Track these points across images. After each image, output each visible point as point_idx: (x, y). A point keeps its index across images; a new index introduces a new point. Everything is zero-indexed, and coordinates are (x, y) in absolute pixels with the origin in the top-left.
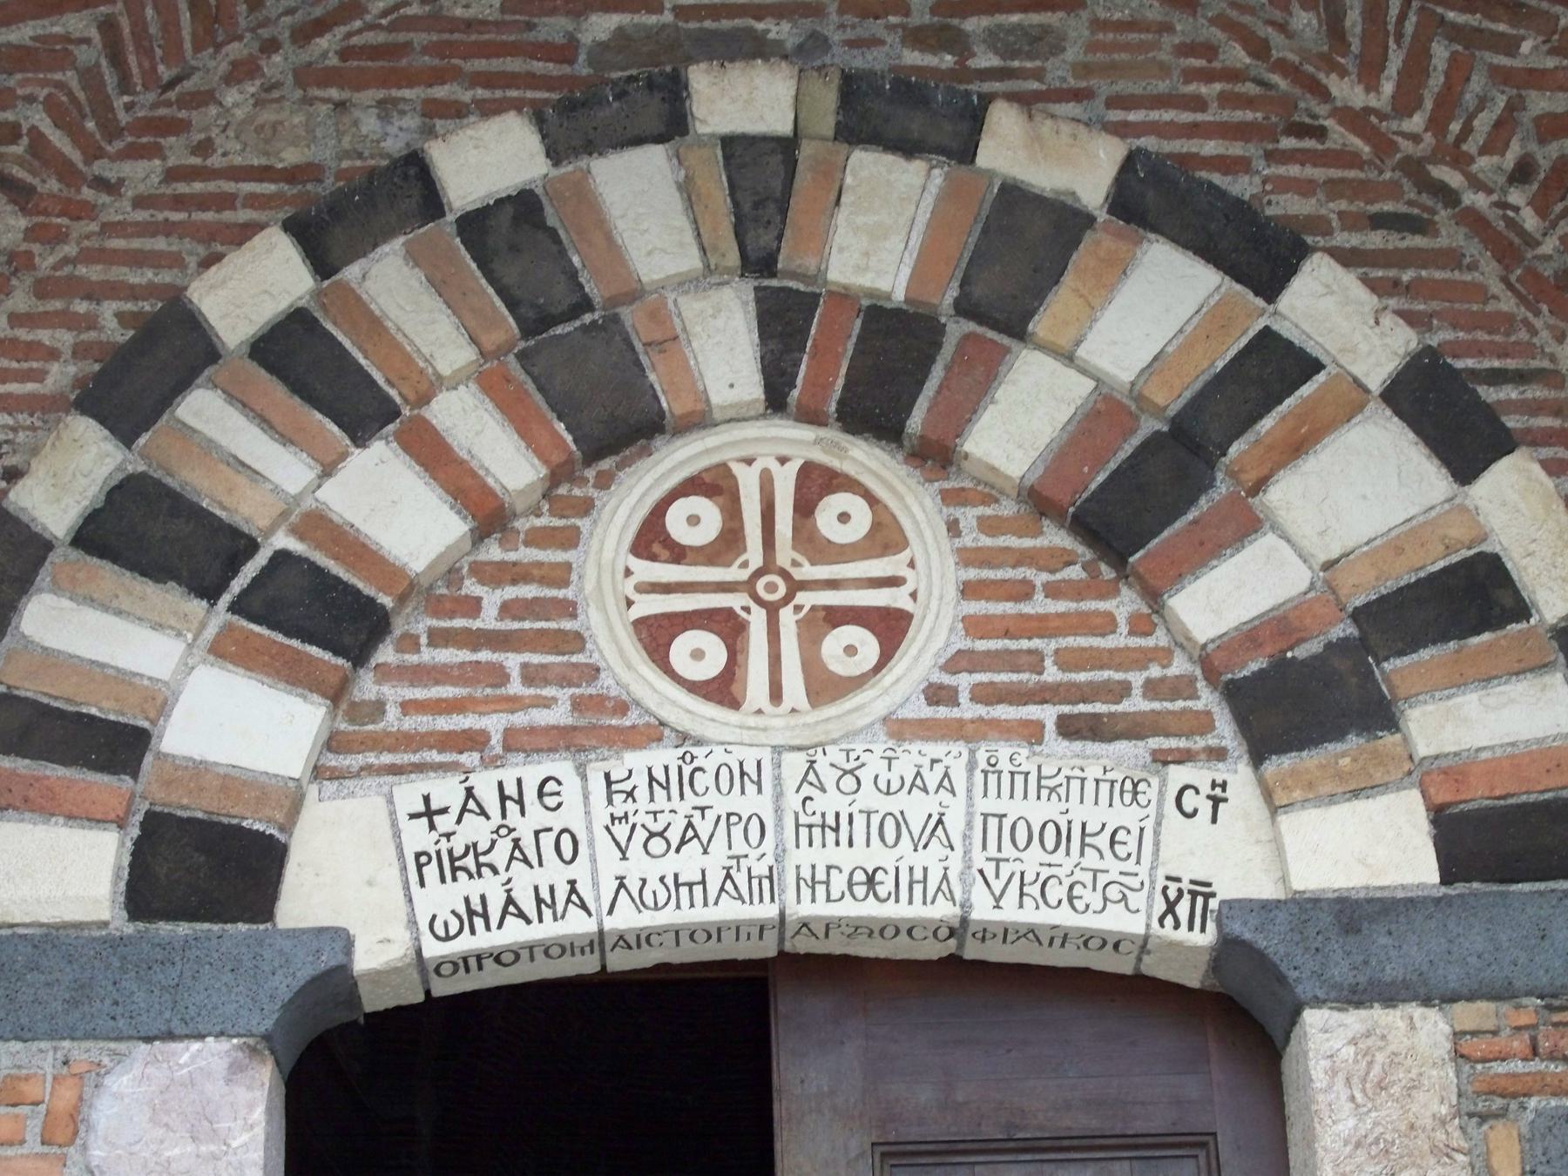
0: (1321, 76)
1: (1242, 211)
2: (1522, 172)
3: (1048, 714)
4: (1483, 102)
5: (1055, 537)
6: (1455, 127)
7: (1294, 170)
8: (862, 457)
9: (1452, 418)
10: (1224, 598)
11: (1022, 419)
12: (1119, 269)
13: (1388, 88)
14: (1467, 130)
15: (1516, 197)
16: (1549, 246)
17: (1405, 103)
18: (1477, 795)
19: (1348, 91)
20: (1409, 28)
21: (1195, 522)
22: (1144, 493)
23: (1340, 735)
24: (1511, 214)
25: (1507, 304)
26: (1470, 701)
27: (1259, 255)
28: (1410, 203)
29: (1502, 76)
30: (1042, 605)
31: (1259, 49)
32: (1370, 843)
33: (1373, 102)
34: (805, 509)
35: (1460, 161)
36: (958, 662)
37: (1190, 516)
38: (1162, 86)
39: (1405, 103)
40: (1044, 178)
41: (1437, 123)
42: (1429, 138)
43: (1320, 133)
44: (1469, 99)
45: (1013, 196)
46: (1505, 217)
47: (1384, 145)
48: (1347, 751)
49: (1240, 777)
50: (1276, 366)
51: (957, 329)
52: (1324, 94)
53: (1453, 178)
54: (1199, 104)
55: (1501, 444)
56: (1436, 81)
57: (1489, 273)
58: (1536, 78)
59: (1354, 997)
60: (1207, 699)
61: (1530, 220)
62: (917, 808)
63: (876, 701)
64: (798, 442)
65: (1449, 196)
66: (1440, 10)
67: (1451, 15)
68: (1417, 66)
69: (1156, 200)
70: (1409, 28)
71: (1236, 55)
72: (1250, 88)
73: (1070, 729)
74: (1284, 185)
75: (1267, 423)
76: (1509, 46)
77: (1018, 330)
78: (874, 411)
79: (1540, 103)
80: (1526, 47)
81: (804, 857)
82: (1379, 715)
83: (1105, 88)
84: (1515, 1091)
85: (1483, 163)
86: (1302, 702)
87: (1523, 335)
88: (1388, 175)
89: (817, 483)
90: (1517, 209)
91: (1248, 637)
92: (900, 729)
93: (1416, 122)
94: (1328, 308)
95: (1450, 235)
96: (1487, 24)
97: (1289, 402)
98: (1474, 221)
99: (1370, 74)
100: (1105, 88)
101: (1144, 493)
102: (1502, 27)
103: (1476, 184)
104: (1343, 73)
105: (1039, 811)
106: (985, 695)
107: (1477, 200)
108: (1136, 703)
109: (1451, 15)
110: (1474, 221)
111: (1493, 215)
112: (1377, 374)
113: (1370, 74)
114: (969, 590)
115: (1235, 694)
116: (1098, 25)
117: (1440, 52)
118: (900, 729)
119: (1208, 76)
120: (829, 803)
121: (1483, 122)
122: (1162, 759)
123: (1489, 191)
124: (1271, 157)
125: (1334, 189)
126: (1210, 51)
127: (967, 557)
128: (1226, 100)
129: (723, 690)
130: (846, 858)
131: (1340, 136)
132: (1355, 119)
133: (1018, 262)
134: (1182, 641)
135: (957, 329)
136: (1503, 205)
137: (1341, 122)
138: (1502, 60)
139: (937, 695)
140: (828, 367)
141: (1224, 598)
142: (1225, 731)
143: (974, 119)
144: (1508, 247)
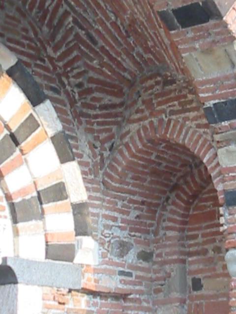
0: (46, 45)
2: (80, 85)
4: (78, 67)
6: (69, 69)
7: (39, 70)
13: (58, 54)
14: (72, 70)
15: (76, 90)
16: (79, 104)
17: (60, 59)
18: (53, 242)
19: (50, 50)
20: (71, 45)
21: (13, 160)
23: (31, 220)
24: (74, 94)
25: (70, 117)
28: (57, 85)
29: (86, 65)
31: (36, 34)
33: (54, 56)
35: (68, 77)
37: (12, 157)
38: (17, 38)
39: (60, 59)
41: (66, 66)
42: (63, 70)
43: (43, 61)
44: (76, 65)
46: (72, 94)
47: (55, 68)
52: (45, 49)
53: (64, 79)
54: (23, 45)
56: (70, 58)
61: (77, 97)
65: (64, 85)
66: (80, 45)
67: (82, 48)
70: (71, 45)
71: (32, 35)
72: (33, 44)
74: (40, 75)
75: (29, 139)
76: (92, 60)
79: (91, 74)
80: (95, 62)
85: (72, 80)
87: (72, 126)
88: (54, 76)
90: (75, 93)
93: (61, 64)
95: (63, 97)
96: (89, 53)
97: (34, 134)
99: (56, 49)
102: (92, 55)
103: (69, 84)
104: (50, 46)
107: (68, 88)
109: (82, 48)
110: (67, 93)
111: (71, 93)
112: (51, 133)
113: (56, 49)
116: (8, 16)
117: (75, 53)
119: (26, 38)
121: (76, 71)
123: (71, 87)
124: (37, 66)
125: (46, 78)
126: (25, 30)
128: (30, 47)
131: (48, 64)
132: (51, 59)
136: (73, 91)
137: (48, 60)
138: (88, 62)
144: (73, 103)
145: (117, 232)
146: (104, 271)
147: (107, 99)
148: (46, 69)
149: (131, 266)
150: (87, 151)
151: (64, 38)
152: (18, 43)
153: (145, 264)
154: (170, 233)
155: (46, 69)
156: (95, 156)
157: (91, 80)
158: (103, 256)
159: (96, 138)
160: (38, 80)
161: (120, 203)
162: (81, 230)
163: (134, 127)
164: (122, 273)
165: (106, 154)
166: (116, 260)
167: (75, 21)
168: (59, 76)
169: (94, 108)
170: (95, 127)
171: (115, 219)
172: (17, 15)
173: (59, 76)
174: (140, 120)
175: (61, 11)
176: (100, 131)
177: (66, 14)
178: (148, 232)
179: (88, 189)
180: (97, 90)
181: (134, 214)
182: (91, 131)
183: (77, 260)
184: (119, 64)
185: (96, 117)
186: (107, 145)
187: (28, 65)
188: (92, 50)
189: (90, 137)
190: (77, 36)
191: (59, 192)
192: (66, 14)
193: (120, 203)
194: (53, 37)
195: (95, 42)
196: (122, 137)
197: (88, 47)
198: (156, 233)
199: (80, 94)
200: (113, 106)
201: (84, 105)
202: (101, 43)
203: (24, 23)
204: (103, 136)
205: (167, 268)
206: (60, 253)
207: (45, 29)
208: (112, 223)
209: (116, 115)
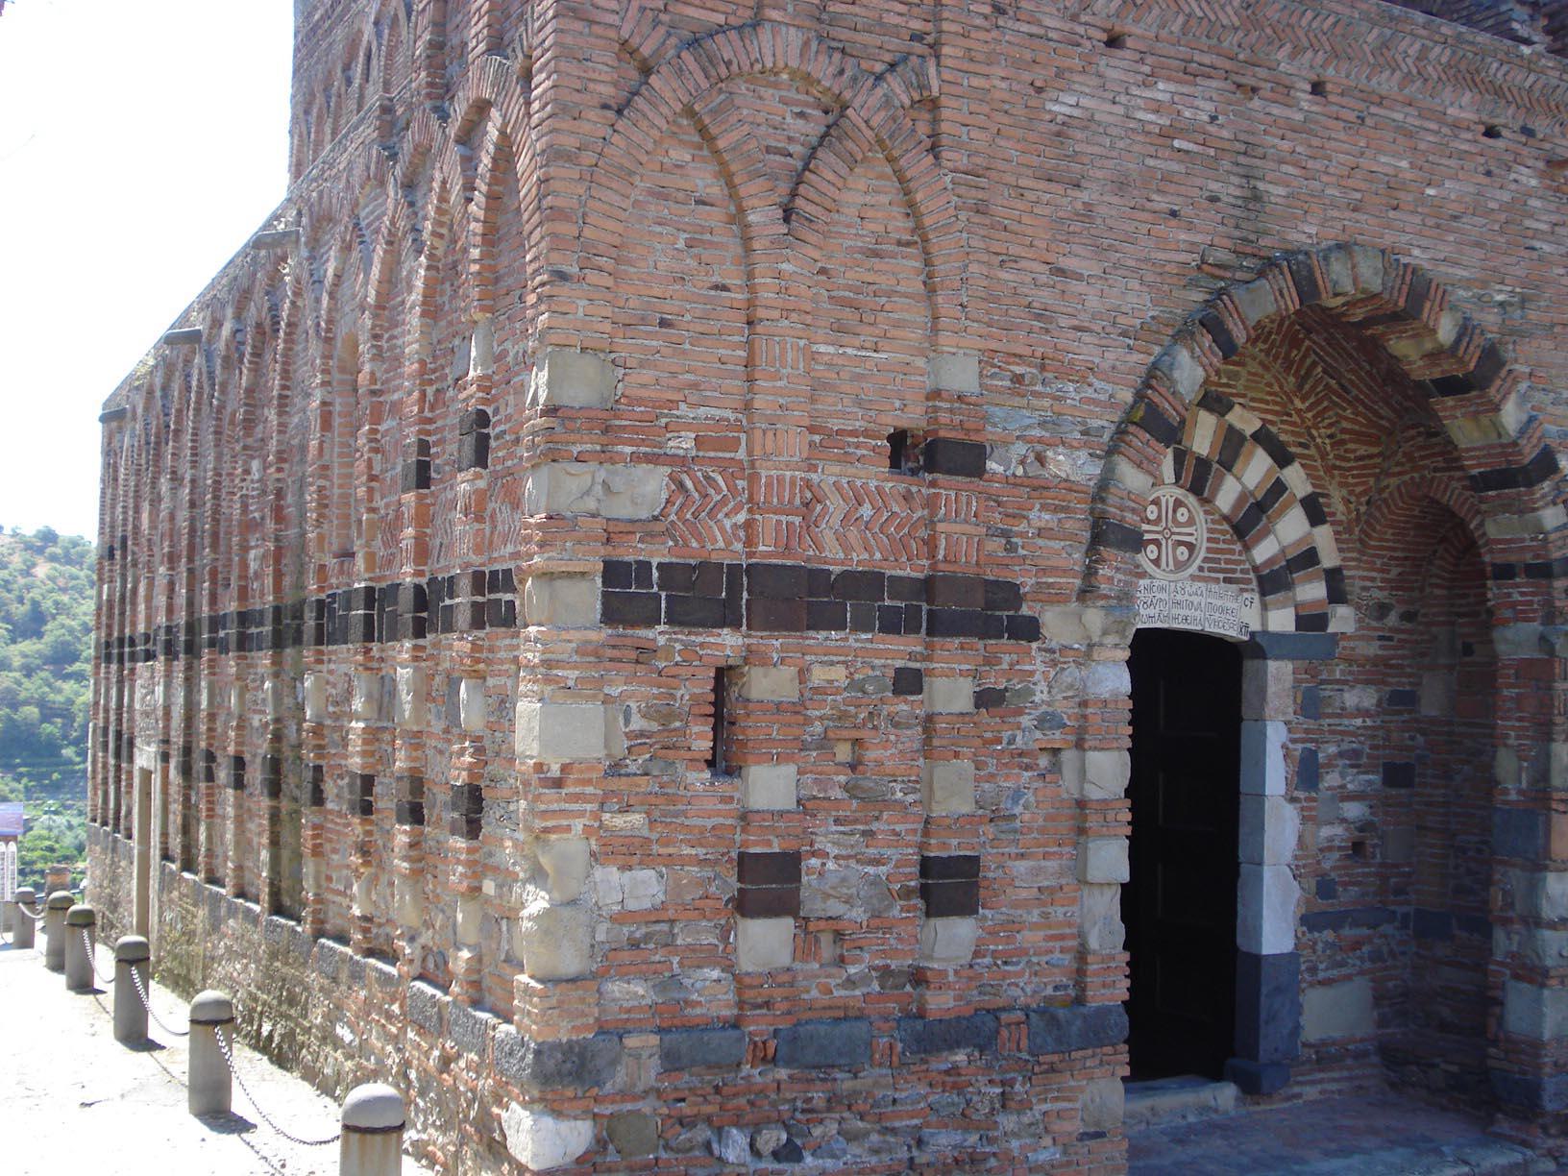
1: (1282, 446)
2: (1330, 436)
3: (1221, 576)
5: (1226, 527)
8: (1191, 500)
9: (1315, 511)
10: (1264, 551)
11: (1227, 495)
12: (1251, 454)
17: (1309, 409)
22: (1249, 520)
26: (1308, 587)
27: (1282, 458)
30: (1222, 546)
31: (1281, 387)
32: (1282, 620)
34: (1175, 511)
36: (1206, 560)
38: (1260, 395)
39: (1309, 409)
40: (1238, 425)
45: (1231, 427)
48: (1280, 596)
49: (1256, 597)
50: (1278, 488)
51: (1216, 466)
54: (1267, 402)
55: (1324, 522)
57: (1318, 463)
58: (1346, 419)
59: (1277, 658)
60: (1252, 575)
62: (1196, 599)
63: (1193, 569)
64: (1179, 493)
65: (1313, 438)
68: (1318, 402)
69: (1262, 438)
71: (1276, 388)
73: (1227, 580)
74: (1286, 432)
77: (1229, 469)
78: (1197, 488)
79: (1345, 424)
81: (1175, 611)
82: (1289, 586)
83: (1250, 394)
84: (1301, 681)
86: (1272, 582)
89: (1178, 504)
91: (1270, 561)
92: (1193, 578)
93: (1309, 415)
94: (1297, 479)
95: (1313, 451)
98: (1317, 446)
100: (1250, 394)
101: (1249, 520)
105: (1219, 603)
106: (1210, 570)
108: (1238, 575)
110: (1317, 446)
112: (1300, 495)
113: (1303, 400)
114: (1209, 540)
115: (1261, 579)
118: (1193, 578)
119: (1270, 394)
120: (1179, 597)
122: (1242, 590)
126: (1269, 385)
127: (1210, 530)
128: (1276, 403)
129: (1156, 562)
130: (1183, 612)
131: (1295, 418)
132: (1299, 411)
133: (1232, 446)
134: (1251, 560)
135: (1216, 466)
139: (1201, 569)
140: (1187, 477)
141: (1264, 551)
142: (1254, 585)
143: (1230, 407)
144: (1324, 456)
145: (1377, 594)
146: (1362, 638)
147: (1362, 450)
148: (1293, 424)
149: (1390, 629)
150: (1341, 508)
151: (1313, 387)
152: (1261, 401)
153: (1408, 626)
154: (1437, 592)
155: (1293, 424)
156: (1350, 512)
157: (1344, 431)
158: (1359, 621)
159: (1351, 493)
160: (1283, 437)
161: (1379, 562)
162: (1336, 595)
163: (1393, 481)
164: (1381, 638)
165: (1363, 509)
166: (1374, 624)
167: (1324, 371)
168: (1308, 428)
169: (1348, 460)
170: (1350, 480)
171: (1373, 579)
172: (1260, 371)
173: (1308, 428)
174: (1400, 474)
175: (1309, 361)
176: (1356, 485)
177: (1314, 364)
178: (1412, 589)
179: (1340, 550)
180: (1351, 441)
181: (1394, 572)
182: (1341, 485)
183: (1330, 630)
184: (1375, 413)
185: (1351, 469)
186: (1363, 499)
187: (1273, 423)
188: (1344, 400)
189: (1344, 492)
190: (1327, 386)
191: (1308, 558)
192: (1314, 364)
193: (1379, 562)
194: (1300, 387)
195: (1348, 392)
196: (1381, 491)
197: (1339, 396)
198: (1422, 589)
199: (1332, 445)
200: (1371, 457)
201: (1337, 457)
202: (1355, 392)
203: (1268, 377)
204: (1358, 489)
205: (1434, 629)
206: (1311, 621)
207: (1292, 379)
208: (1368, 584)
209: (1375, 466)
